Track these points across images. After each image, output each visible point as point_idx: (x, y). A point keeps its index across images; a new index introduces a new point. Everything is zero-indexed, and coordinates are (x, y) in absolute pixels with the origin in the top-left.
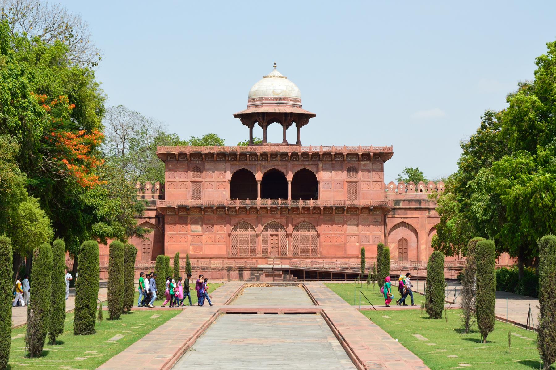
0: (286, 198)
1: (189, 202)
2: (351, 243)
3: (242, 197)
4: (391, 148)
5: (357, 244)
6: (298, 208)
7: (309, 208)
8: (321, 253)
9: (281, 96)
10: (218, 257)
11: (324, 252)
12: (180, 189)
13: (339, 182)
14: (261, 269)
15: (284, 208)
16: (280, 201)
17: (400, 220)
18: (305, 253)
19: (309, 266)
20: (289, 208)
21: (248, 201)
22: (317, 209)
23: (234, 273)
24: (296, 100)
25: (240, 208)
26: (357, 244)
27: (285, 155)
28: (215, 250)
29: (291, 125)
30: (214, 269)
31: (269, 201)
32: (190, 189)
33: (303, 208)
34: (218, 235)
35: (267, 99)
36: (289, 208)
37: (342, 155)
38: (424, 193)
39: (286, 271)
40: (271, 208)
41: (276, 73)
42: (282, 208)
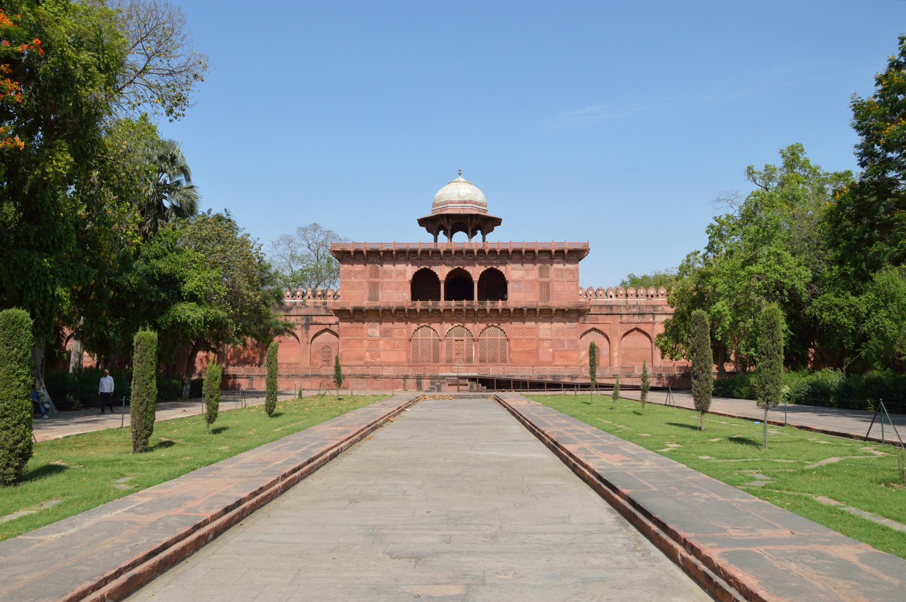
0: (472, 299)
1: (366, 304)
2: (550, 348)
3: (424, 298)
4: (587, 245)
5: (551, 350)
6: (485, 310)
7: (497, 310)
8: (511, 360)
9: (466, 199)
10: (397, 364)
11: (514, 359)
12: (352, 287)
13: (530, 282)
14: (443, 377)
15: (470, 311)
16: (465, 302)
17: (591, 326)
18: (493, 360)
19: (501, 374)
20: (476, 310)
21: (430, 303)
22: (506, 310)
23: (411, 382)
24: (481, 204)
25: (421, 310)
26: (551, 350)
27: (470, 252)
28: (393, 357)
29: (476, 234)
30: (386, 377)
31: (453, 303)
32: (368, 291)
33: (491, 310)
34: (397, 339)
35: (452, 202)
36: (476, 310)
37: (533, 252)
38: (614, 298)
39: (473, 379)
40: (456, 310)
41: (461, 179)
42: (468, 310)
